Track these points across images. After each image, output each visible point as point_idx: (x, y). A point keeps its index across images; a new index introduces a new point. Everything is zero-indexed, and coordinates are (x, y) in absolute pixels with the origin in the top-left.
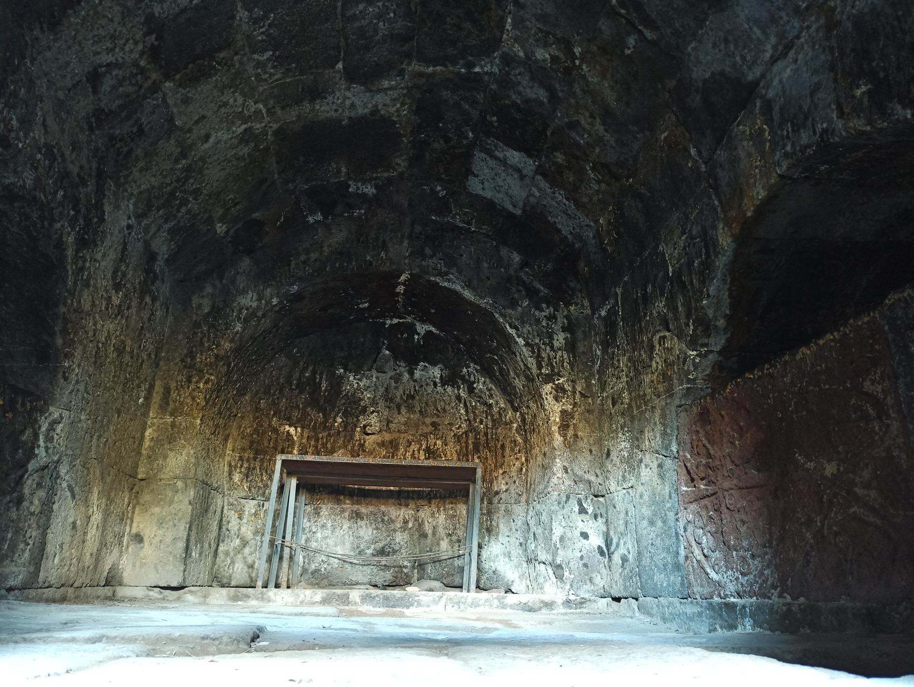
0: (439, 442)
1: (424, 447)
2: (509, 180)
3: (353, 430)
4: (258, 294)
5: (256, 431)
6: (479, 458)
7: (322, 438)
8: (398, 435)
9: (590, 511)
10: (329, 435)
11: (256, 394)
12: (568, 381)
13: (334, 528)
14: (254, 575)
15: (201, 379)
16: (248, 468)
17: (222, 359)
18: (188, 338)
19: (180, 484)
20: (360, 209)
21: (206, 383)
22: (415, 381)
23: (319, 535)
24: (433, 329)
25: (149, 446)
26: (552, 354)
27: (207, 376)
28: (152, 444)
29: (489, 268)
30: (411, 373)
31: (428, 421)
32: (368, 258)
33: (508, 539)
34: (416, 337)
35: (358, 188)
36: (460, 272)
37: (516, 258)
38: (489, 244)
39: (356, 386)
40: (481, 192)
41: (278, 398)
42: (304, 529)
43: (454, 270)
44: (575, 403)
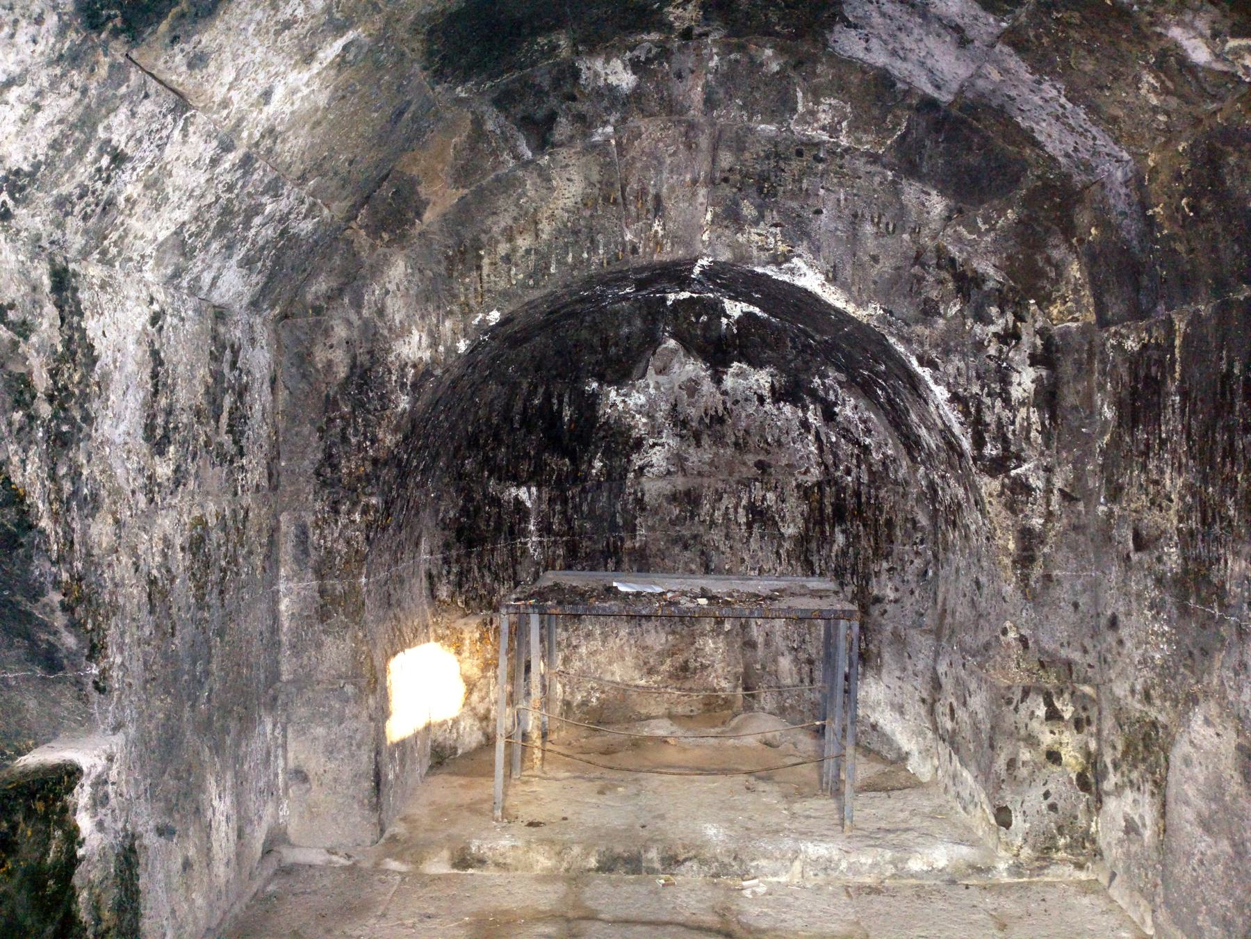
0: (770, 496)
1: (744, 502)
2: (931, 42)
3: (623, 477)
4: (431, 334)
5: (464, 511)
6: (843, 532)
7: (573, 498)
8: (699, 480)
9: (1067, 716)
10: (584, 490)
11: (455, 457)
12: (1037, 467)
13: (605, 636)
14: (490, 730)
15: (355, 504)
16: (460, 574)
17: (386, 464)
18: (320, 430)
19: (349, 689)
20: (605, 123)
21: (365, 512)
22: (725, 393)
23: (583, 650)
24: (757, 310)
25: (290, 629)
26: (1007, 414)
27: (364, 500)
28: (294, 625)
29: (878, 235)
30: (718, 380)
31: (751, 459)
32: (629, 237)
33: (900, 683)
34: (724, 321)
35: (597, 75)
36: (816, 250)
37: (937, 205)
38: (877, 179)
39: (621, 406)
40: (861, 55)
41: (493, 449)
42: (559, 643)
43: (802, 249)
44: (1050, 514)
